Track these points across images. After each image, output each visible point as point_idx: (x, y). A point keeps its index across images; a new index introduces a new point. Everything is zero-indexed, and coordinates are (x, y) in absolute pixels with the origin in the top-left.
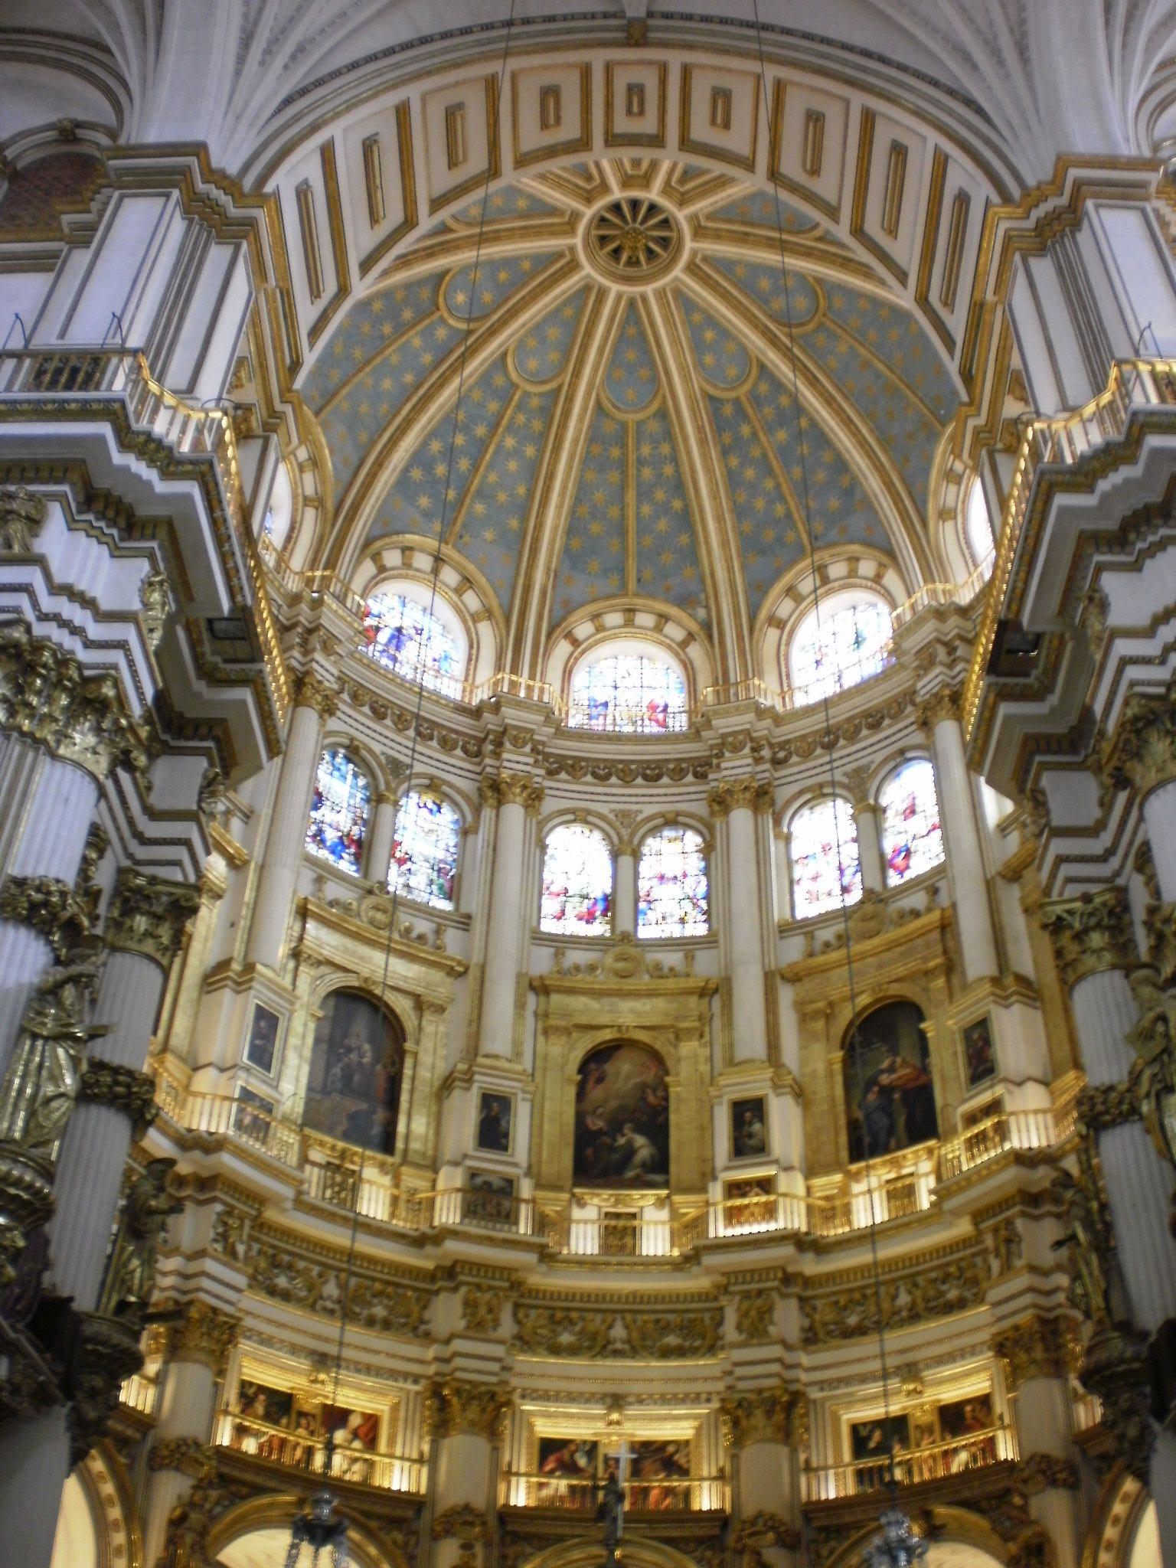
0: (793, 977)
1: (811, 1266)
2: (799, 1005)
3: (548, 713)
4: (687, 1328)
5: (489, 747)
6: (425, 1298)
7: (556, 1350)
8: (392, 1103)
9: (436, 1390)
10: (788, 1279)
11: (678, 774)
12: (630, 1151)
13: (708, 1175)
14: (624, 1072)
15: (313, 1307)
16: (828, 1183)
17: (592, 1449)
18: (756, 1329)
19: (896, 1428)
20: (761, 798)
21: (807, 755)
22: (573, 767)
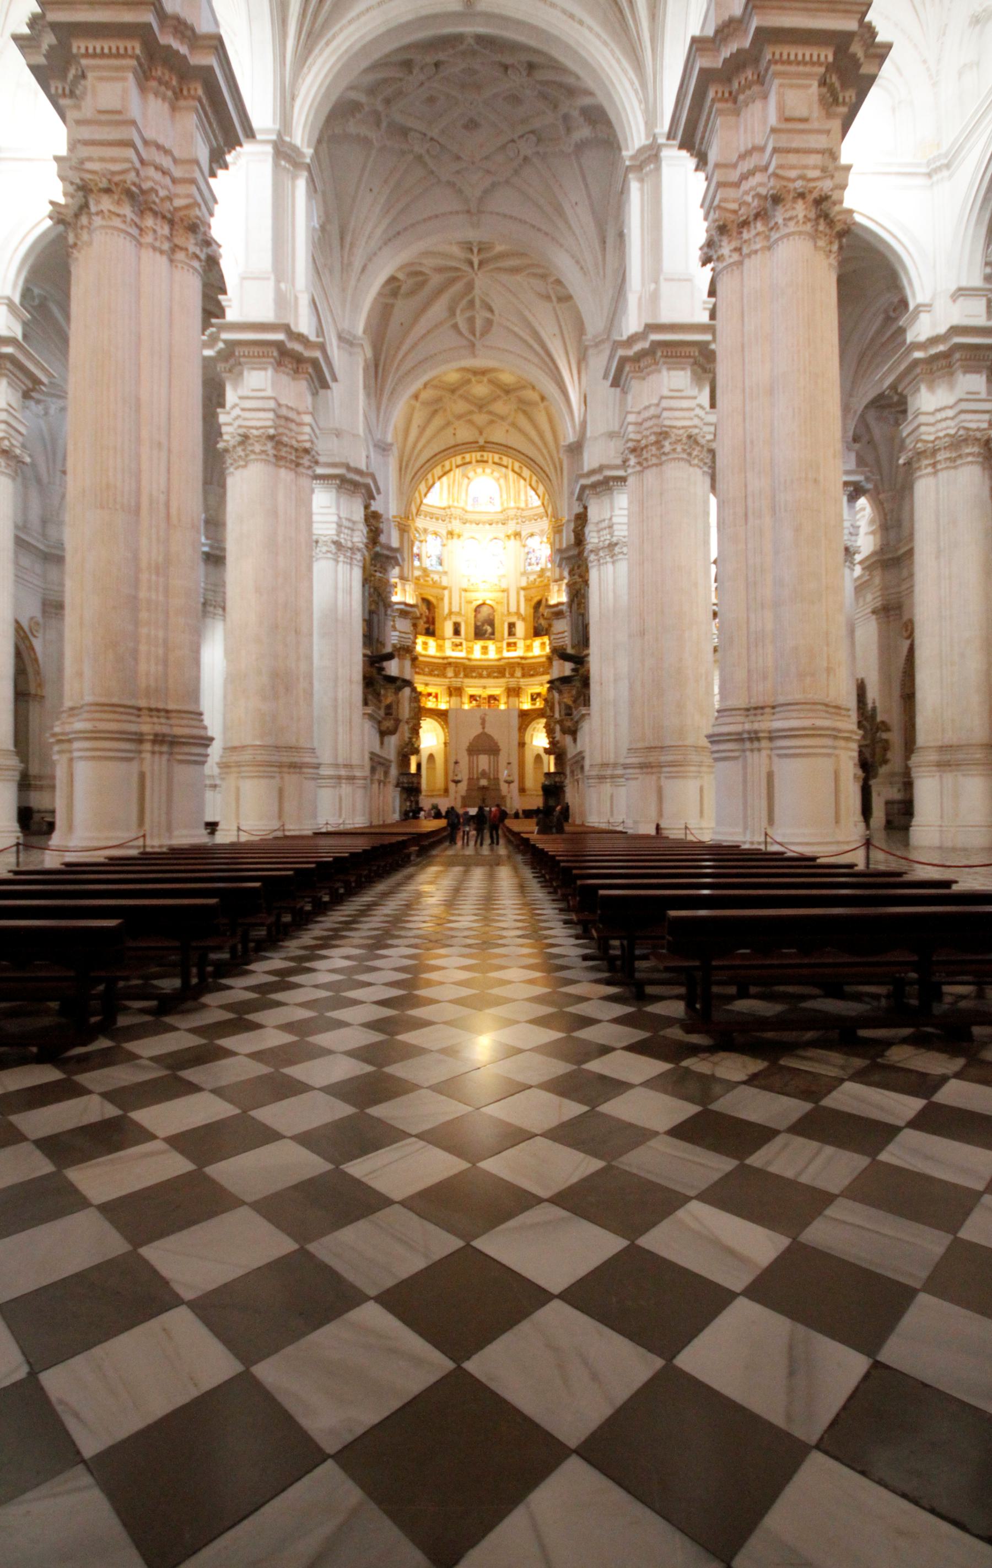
0: (524, 589)
1: (523, 661)
2: (525, 596)
3: (463, 509)
4: (499, 672)
5: (448, 520)
6: (445, 668)
7: (472, 677)
8: (433, 623)
9: (449, 688)
10: (519, 664)
11: (497, 523)
12: (486, 631)
13: (503, 639)
14: (485, 611)
15: (424, 674)
16: (529, 642)
17: (480, 696)
18: (512, 675)
19: (539, 695)
20: (517, 535)
21: (530, 520)
22: (471, 522)
